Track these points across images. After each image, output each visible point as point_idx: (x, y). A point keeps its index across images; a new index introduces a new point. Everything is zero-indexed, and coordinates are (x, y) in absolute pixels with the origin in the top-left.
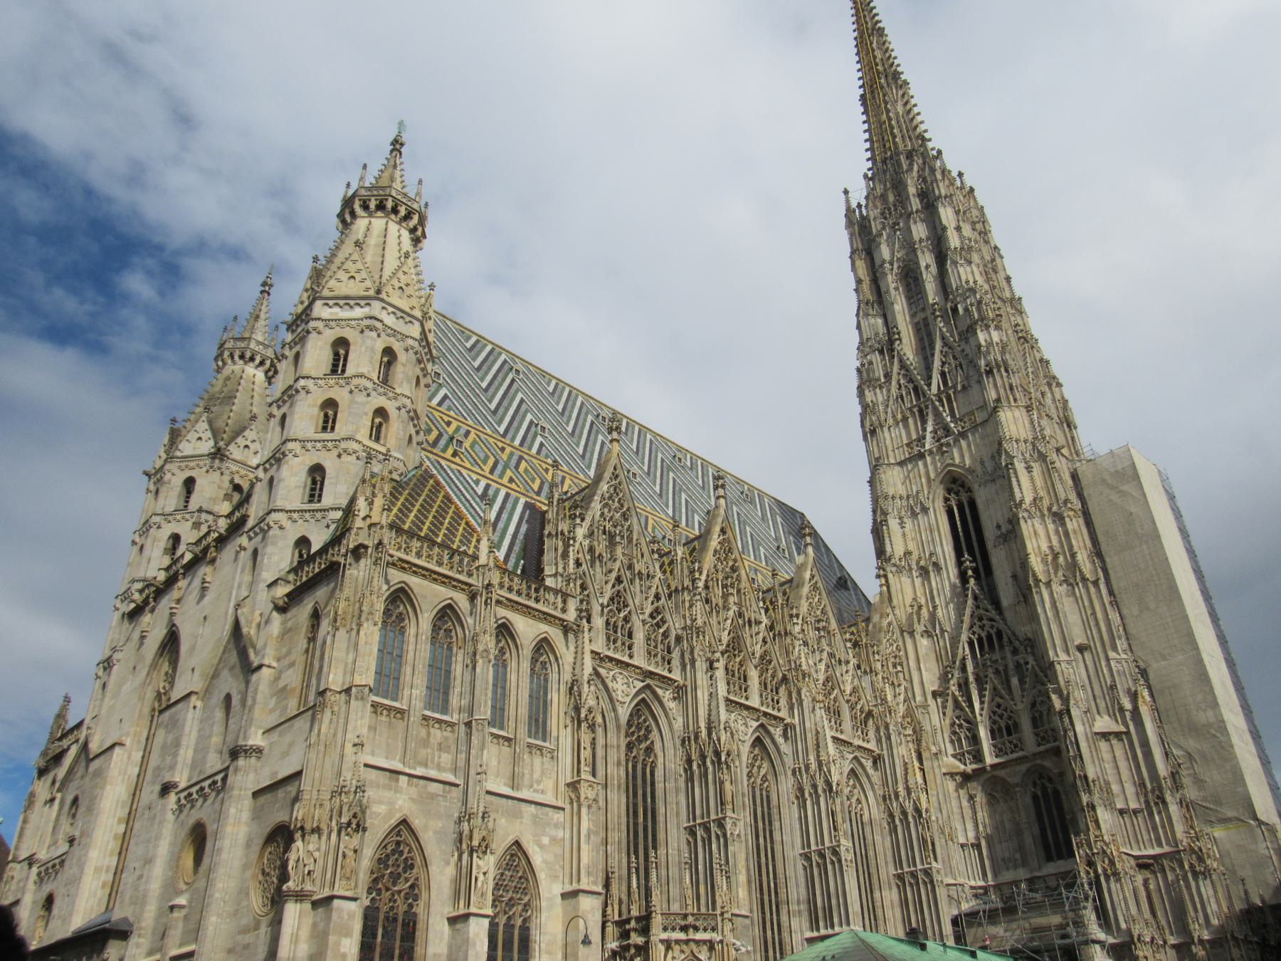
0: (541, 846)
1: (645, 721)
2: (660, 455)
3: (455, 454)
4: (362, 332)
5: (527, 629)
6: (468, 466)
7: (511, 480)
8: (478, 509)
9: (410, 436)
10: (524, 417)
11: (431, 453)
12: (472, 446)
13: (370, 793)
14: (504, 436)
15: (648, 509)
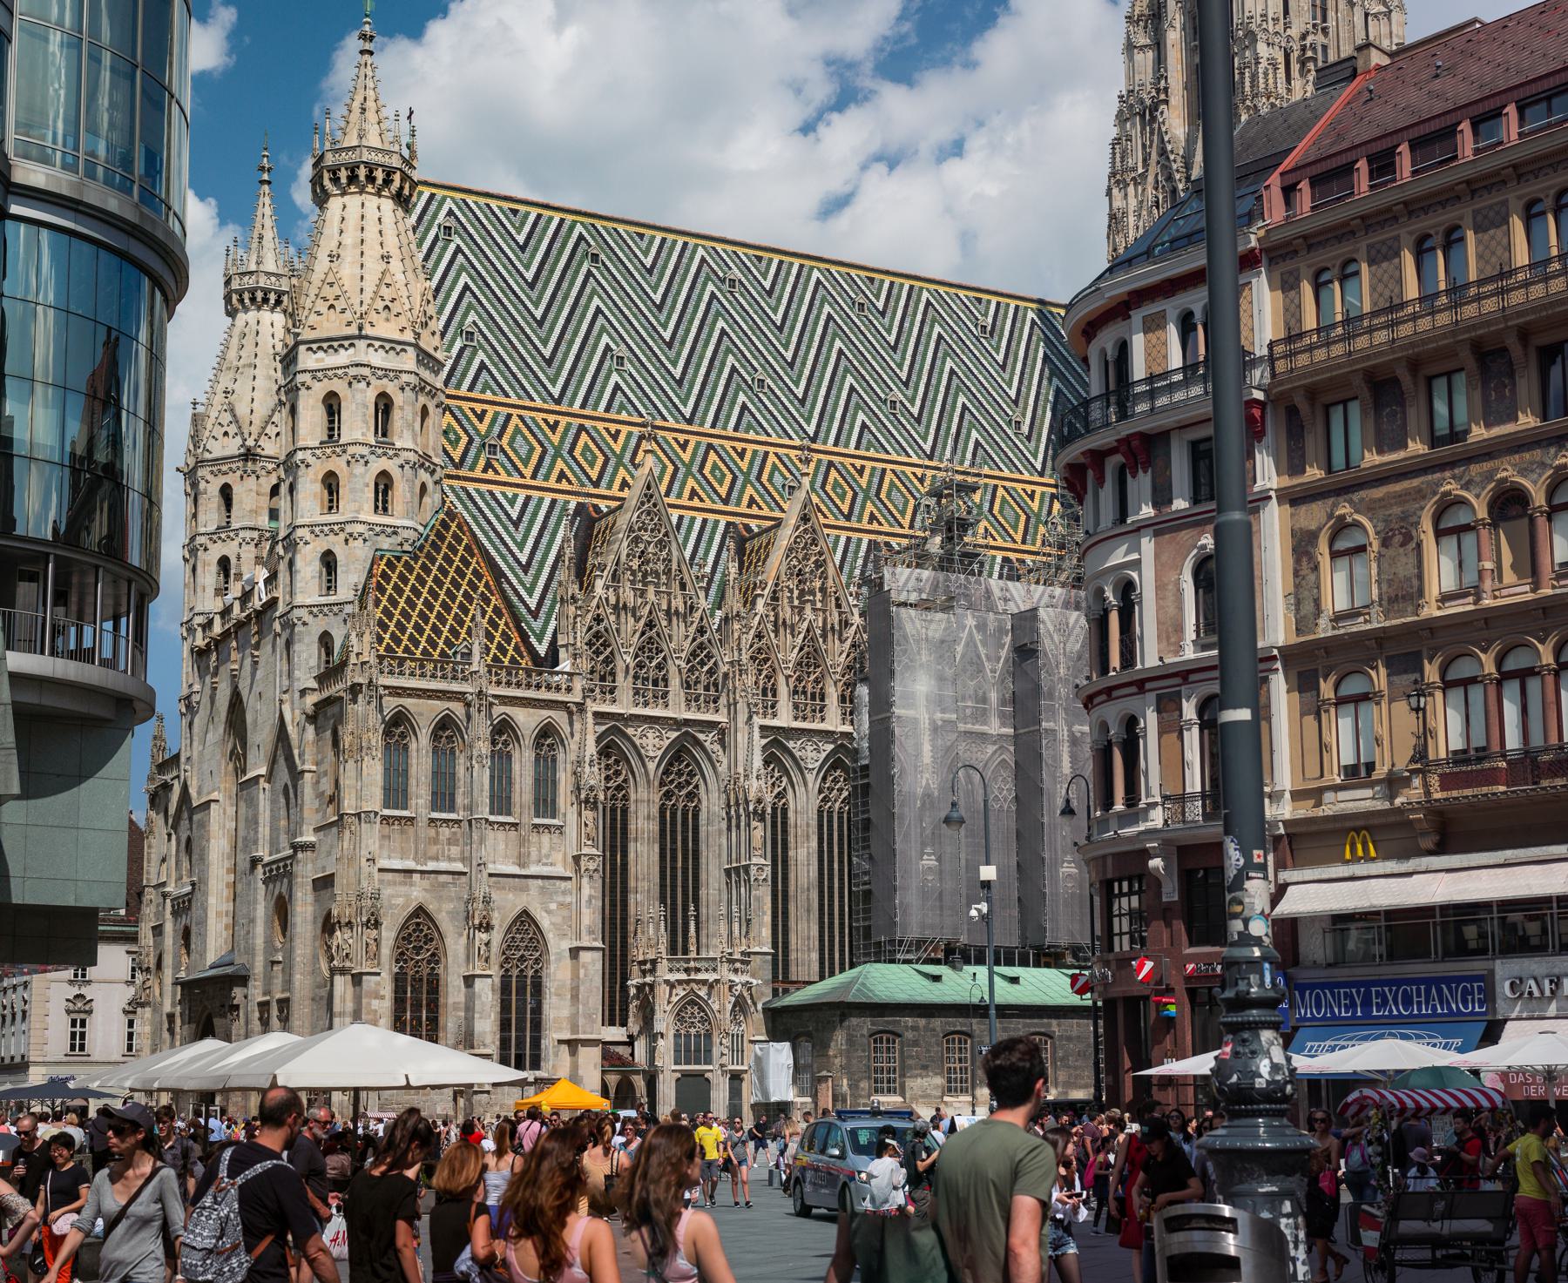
0: (549, 912)
1: (688, 765)
2: (827, 309)
3: (488, 466)
4: (350, 384)
5: (527, 720)
6: (503, 477)
7: (562, 476)
8: (510, 543)
9: (423, 487)
10: (596, 346)
11: (458, 478)
12: (511, 444)
13: (387, 892)
14: (558, 402)
15: (774, 439)
